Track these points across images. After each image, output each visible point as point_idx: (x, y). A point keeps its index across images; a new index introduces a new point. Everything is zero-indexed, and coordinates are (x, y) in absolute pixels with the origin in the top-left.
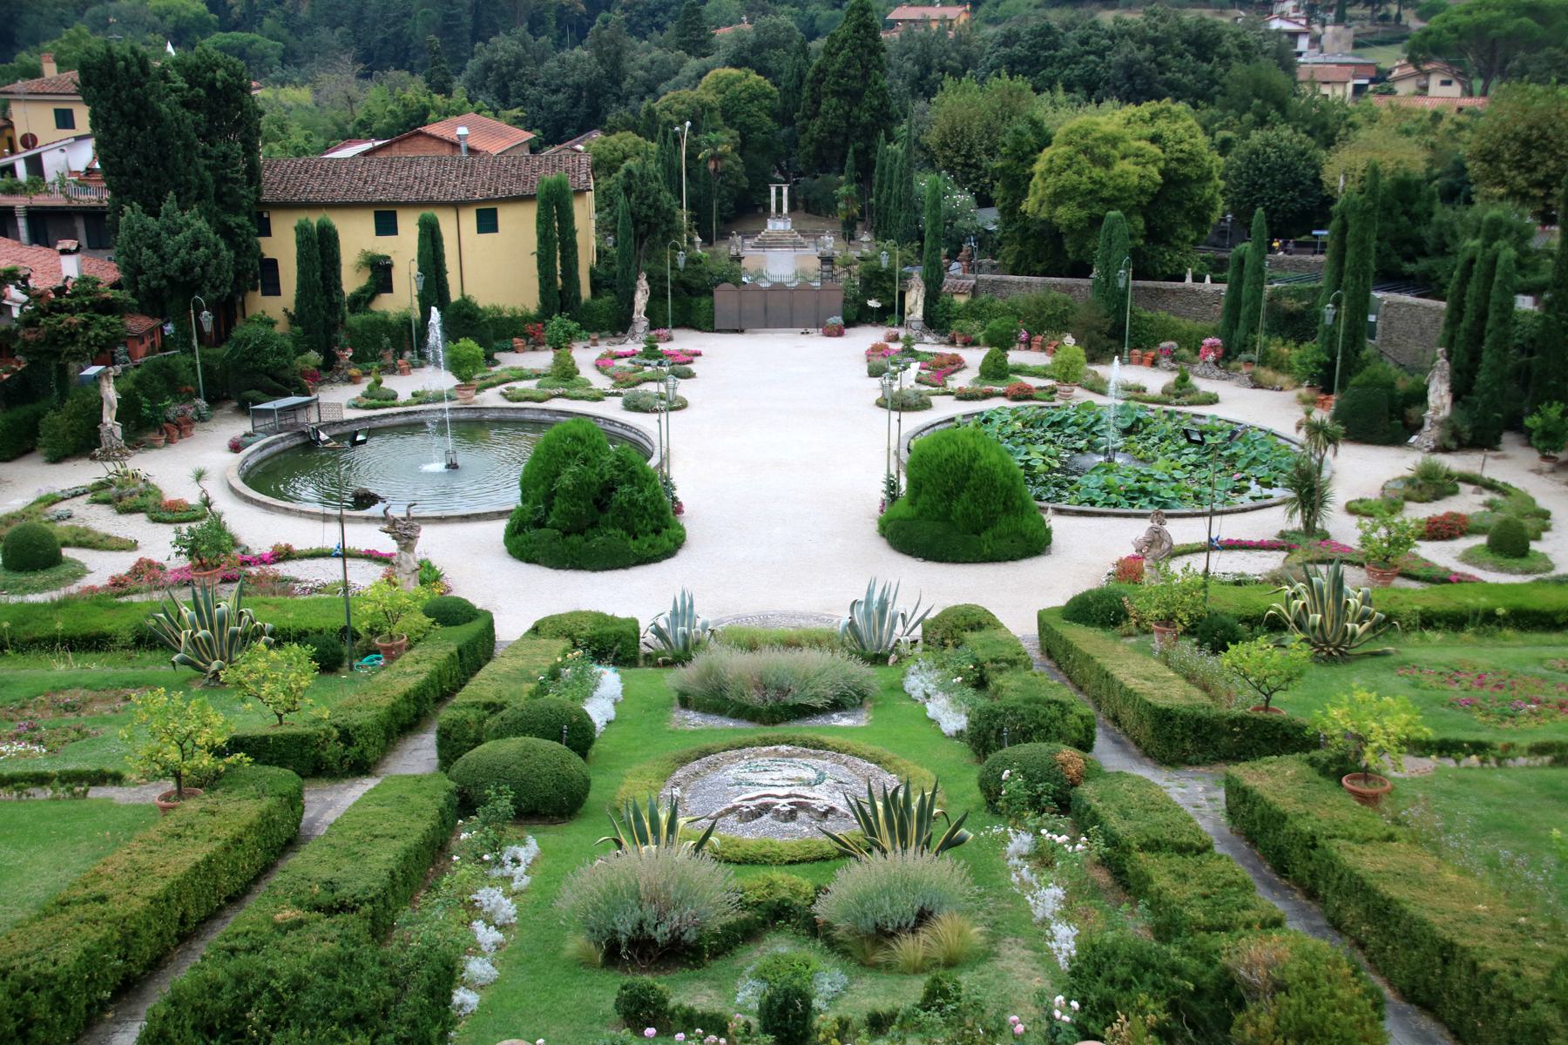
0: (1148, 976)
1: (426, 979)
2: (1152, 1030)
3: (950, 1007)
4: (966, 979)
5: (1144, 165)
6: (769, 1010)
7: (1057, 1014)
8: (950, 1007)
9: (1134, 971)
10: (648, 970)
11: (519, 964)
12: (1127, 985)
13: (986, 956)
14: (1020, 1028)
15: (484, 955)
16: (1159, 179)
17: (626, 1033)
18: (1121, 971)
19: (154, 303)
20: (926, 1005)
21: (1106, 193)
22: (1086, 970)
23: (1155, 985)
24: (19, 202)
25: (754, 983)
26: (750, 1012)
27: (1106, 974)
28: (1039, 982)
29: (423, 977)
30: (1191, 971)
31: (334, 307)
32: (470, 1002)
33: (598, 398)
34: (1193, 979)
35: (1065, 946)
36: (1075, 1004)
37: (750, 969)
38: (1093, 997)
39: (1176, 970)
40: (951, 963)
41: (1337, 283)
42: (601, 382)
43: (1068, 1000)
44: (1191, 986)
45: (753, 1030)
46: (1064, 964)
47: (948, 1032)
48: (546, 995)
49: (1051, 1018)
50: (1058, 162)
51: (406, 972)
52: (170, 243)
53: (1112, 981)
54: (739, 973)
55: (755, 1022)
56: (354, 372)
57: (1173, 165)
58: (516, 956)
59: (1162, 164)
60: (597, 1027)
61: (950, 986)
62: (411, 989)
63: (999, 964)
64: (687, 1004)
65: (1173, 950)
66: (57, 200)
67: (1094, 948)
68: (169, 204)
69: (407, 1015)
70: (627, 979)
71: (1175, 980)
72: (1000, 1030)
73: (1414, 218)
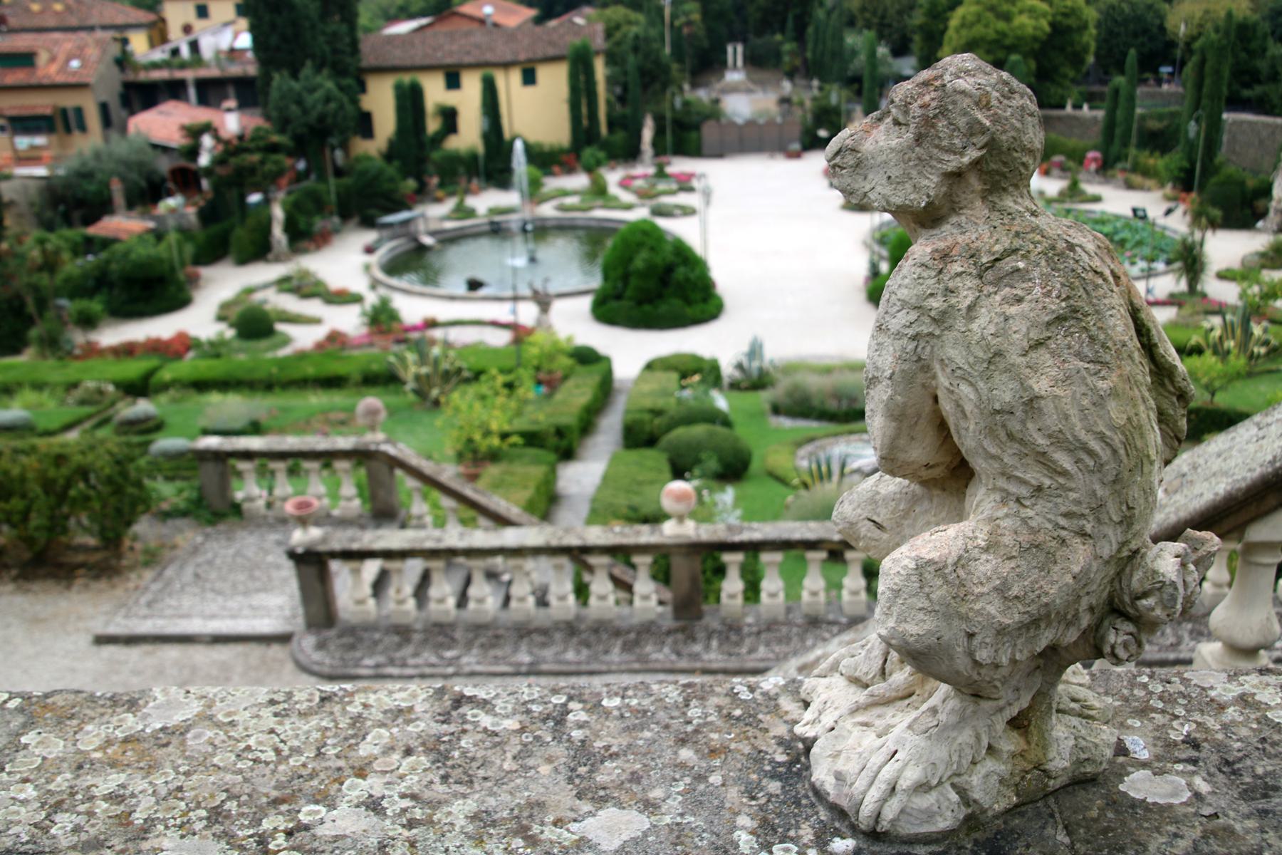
5: (1036, 19)
16: (1048, 29)
19: (300, 148)
21: (1008, 42)
24: (189, 75)
31: (421, 145)
33: (629, 207)
41: (1197, 105)
42: (626, 197)
50: (970, 18)
52: (310, 99)
56: (440, 193)
57: (1059, 18)
59: (1050, 18)
66: (214, 72)
68: (307, 70)
73: (1252, 54)
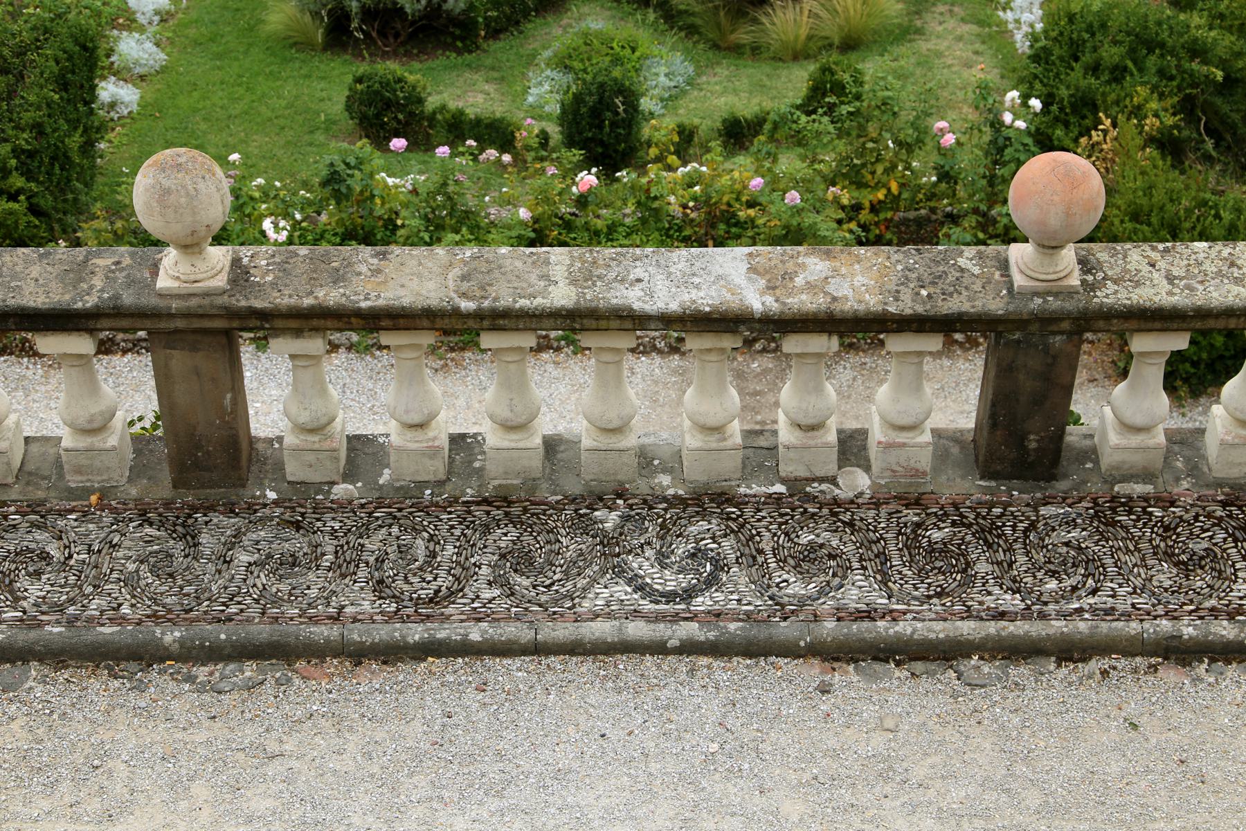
0: (1152, 62)
1: (52, 63)
2: (1151, 140)
3: (845, 109)
4: (872, 67)
6: (576, 112)
7: (1008, 118)
8: (845, 109)
9: (1132, 52)
10: (395, 55)
11: (196, 43)
12: (1118, 74)
13: (905, 33)
14: (949, 139)
15: (141, 29)
17: (363, 147)
18: (1111, 54)
20: (809, 106)
22: (1057, 51)
23: (1161, 73)
25: (554, 74)
26: (548, 117)
27: (1087, 58)
28: (984, 70)
29: (46, 61)
30: (1221, 51)
32: (127, 99)
34: (1223, 64)
35: (1026, 17)
36: (1036, 104)
37: (547, 54)
38: (1064, 92)
39: (1197, 51)
40: (850, 44)
43: (1025, 97)
44: (1219, 75)
45: (552, 143)
46: (1022, 44)
47: (841, 146)
48: (241, 91)
49: (997, 125)
51: (21, 53)
53: (1095, 69)
54: (531, 60)
55: (554, 131)
58: (192, 32)
60: (320, 137)
61: (846, 78)
62: (30, 78)
63: (923, 46)
64: (453, 105)
65: (1196, 19)
67: (1071, 18)
69: (28, 117)
70: (363, 68)
71: (1195, 66)
72: (920, 142)
